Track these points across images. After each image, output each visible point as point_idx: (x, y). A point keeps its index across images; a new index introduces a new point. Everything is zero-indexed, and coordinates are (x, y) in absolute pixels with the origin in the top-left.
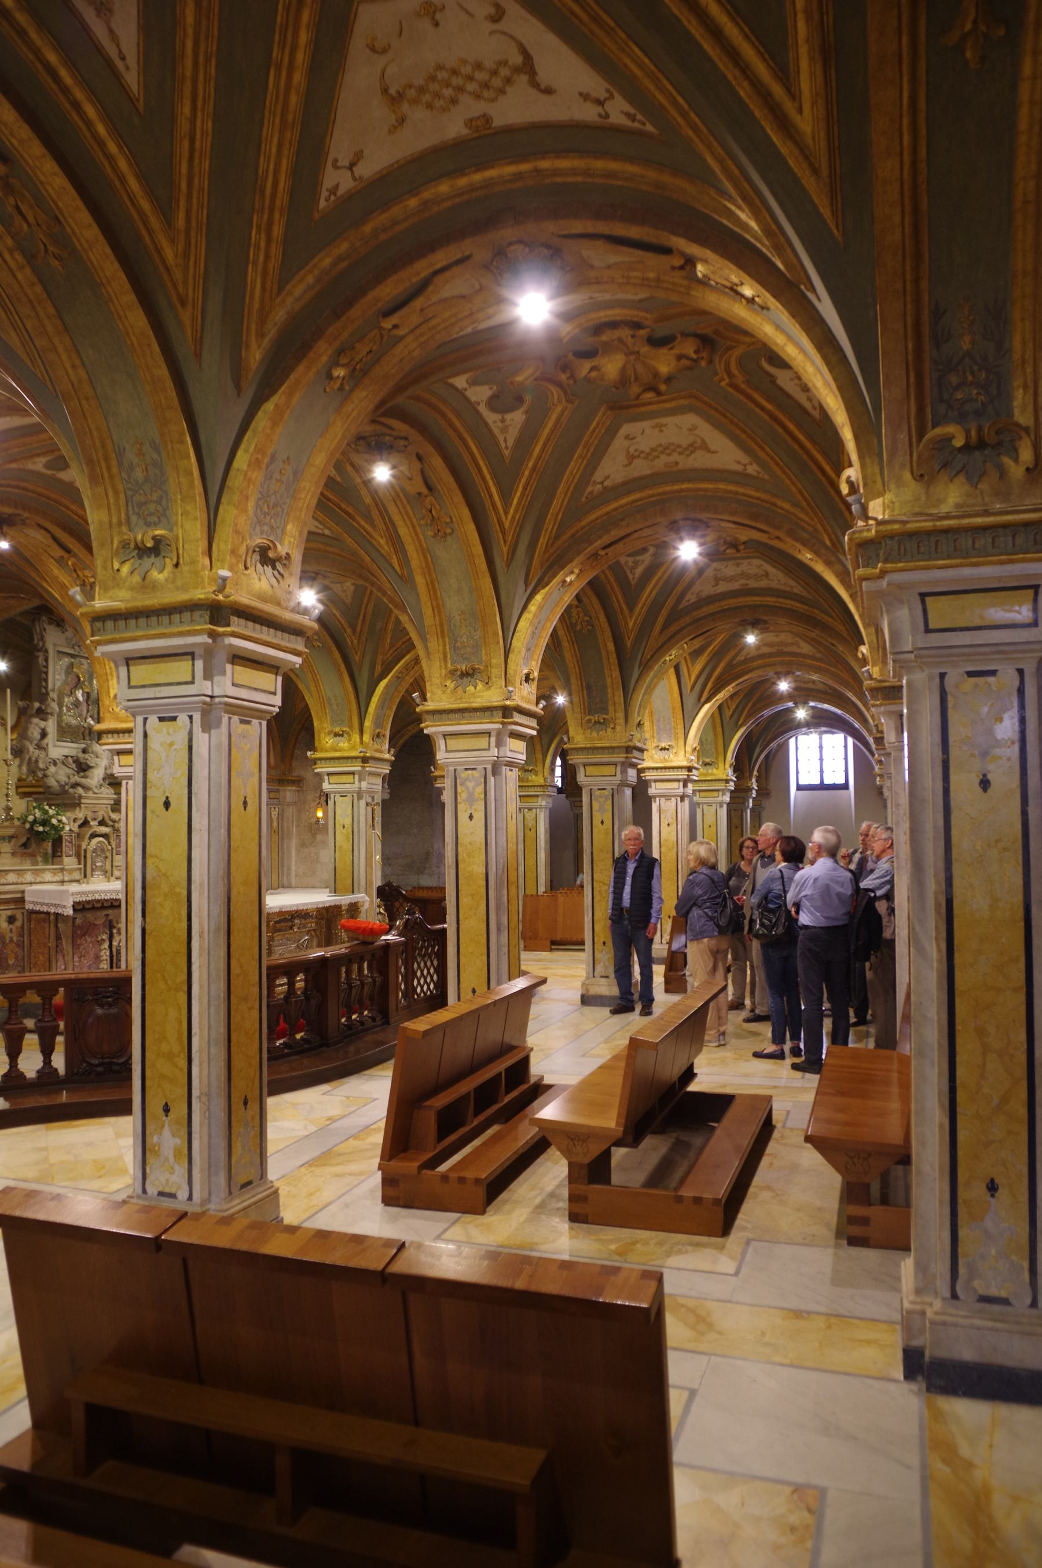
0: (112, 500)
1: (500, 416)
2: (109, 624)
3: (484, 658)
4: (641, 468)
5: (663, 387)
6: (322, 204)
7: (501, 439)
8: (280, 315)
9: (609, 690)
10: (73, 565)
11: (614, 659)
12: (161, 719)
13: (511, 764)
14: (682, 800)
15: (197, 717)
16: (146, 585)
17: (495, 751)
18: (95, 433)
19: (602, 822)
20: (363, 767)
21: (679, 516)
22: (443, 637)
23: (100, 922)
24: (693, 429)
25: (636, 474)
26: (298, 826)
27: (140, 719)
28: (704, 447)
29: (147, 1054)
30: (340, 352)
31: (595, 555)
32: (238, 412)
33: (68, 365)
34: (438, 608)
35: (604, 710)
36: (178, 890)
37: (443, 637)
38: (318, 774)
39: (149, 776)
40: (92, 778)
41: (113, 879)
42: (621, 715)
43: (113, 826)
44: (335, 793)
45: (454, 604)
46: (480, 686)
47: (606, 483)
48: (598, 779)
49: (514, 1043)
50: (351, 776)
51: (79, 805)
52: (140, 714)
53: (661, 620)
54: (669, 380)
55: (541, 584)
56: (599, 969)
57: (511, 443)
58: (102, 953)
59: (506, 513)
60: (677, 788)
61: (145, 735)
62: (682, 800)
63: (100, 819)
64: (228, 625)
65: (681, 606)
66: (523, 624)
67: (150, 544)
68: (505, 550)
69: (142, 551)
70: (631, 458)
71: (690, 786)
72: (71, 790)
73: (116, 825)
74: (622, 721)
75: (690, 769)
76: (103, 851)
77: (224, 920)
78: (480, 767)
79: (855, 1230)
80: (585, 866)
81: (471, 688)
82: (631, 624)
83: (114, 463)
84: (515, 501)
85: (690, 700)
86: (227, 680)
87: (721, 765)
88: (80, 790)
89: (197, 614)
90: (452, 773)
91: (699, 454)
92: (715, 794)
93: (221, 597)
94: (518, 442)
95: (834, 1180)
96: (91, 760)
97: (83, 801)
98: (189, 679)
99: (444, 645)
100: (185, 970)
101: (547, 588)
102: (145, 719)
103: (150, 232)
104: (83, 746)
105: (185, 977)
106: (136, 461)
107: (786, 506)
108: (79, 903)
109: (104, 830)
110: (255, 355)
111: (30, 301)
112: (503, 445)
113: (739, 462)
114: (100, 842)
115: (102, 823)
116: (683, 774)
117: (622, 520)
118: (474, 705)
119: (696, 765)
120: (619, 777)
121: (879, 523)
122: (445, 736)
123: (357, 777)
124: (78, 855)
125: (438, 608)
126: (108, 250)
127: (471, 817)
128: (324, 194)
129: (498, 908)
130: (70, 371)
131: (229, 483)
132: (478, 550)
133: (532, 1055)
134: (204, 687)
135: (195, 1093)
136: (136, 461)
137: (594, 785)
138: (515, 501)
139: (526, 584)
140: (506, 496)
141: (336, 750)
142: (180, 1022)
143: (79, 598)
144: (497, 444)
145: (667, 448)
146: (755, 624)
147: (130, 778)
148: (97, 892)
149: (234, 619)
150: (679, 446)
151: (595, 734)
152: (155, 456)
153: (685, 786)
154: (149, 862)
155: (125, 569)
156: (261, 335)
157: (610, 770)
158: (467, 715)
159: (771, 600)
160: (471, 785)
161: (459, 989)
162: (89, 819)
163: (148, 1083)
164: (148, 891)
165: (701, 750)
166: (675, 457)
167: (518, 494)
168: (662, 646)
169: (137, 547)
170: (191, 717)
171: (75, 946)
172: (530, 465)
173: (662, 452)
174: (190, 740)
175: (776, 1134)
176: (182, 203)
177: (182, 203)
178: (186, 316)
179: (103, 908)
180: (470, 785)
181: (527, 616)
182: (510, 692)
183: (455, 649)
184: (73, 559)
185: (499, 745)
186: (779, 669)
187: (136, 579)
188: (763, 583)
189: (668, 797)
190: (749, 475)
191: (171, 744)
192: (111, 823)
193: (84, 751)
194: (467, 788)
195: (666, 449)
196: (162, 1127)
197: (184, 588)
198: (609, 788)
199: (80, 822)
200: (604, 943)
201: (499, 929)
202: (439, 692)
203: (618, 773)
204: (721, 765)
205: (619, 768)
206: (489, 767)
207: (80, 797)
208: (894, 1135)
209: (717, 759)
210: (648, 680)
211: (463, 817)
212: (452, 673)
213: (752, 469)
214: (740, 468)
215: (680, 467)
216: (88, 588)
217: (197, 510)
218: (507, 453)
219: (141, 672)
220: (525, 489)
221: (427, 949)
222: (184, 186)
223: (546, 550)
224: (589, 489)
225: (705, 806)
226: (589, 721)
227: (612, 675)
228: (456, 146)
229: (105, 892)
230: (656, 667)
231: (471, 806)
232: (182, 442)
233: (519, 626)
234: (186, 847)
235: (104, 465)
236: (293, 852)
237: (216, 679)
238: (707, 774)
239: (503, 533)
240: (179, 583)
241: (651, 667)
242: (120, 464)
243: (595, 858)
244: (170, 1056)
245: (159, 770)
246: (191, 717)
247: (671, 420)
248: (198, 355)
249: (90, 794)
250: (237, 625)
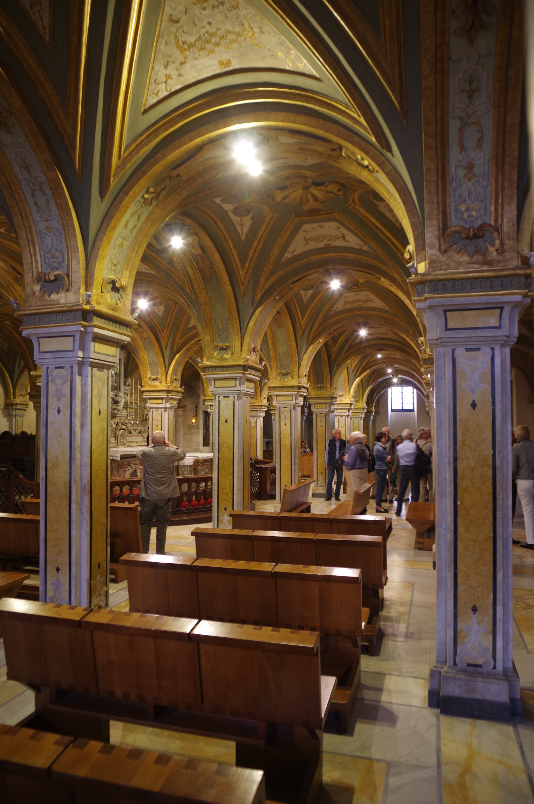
0: (211, 333)
1: (305, 292)
2: (210, 369)
3: (291, 369)
4: (349, 306)
5: (360, 285)
6: (283, 260)
7: (304, 298)
8: (266, 287)
9: (325, 375)
10: (141, 331)
11: (327, 363)
12: (224, 397)
13: (299, 406)
14: (348, 417)
15: (236, 397)
16: (223, 359)
17: (294, 401)
18: (209, 315)
19: (321, 426)
21: (360, 320)
22: (277, 361)
23: (126, 463)
24: (368, 295)
25: (347, 308)
26: (183, 426)
27: (217, 397)
28: (371, 301)
29: (219, 493)
30: (278, 294)
31: (330, 333)
32: (252, 311)
33: (204, 297)
34: (275, 351)
35: (323, 383)
36: (230, 446)
37: (277, 361)
39: (221, 413)
40: (120, 406)
42: (329, 385)
45: (281, 350)
46: (290, 378)
47: (337, 311)
48: (320, 409)
49: (305, 501)
52: (217, 395)
53: (346, 349)
54: (362, 284)
55: (312, 343)
56: (319, 483)
57: (307, 299)
58: (126, 475)
59: (302, 320)
60: (346, 412)
61: (219, 401)
62: (348, 417)
64: (247, 371)
65: (353, 344)
66: (305, 357)
67: (225, 347)
68: (301, 332)
69: (221, 349)
70: (346, 303)
71: (351, 411)
74: (329, 387)
75: (351, 404)
76: (123, 435)
77: (243, 455)
78: (289, 407)
79: (420, 546)
80: (314, 443)
81: (286, 379)
82: (334, 350)
83: (213, 323)
84: (306, 317)
85: (352, 376)
86: (245, 386)
87: (361, 402)
88: (116, 411)
89: (239, 368)
90: (278, 409)
91: (369, 302)
92: (358, 414)
93: (246, 363)
94: (310, 298)
95: (415, 532)
96: (119, 400)
97: (117, 415)
98: (235, 386)
99: (277, 364)
100: (232, 469)
101: (314, 345)
102: (219, 397)
103: (237, 268)
104: (115, 393)
105: (232, 471)
106: (220, 323)
107: (397, 320)
108: (123, 455)
109: (124, 427)
110: (258, 297)
111: (198, 281)
112: (304, 299)
113: (382, 306)
114: (122, 432)
115: (123, 424)
116: (348, 406)
117: (341, 322)
118: (288, 385)
119: (353, 403)
120: (328, 409)
121: (429, 355)
122: (276, 396)
124: (115, 437)
125: (275, 351)
126: (226, 272)
127: (285, 424)
128: (284, 258)
129: (295, 457)
130: (205, 299)
131: (247, 330)
132: (292, 332)
133: (312, 505)
134: (238, 388)
135: (235, 504)
136: (220, 323)
138: (306, 317)
139: (307, 343)
140: (303, 315)
142: (230, 483)
143: (200, 361)
144: (302, 299)
145: (359, 300)
146: (380, 350)
147: (212, 413)
148: (127, 451)
149: (249, 369)
150: (362, 300)
151: (319, 392)
152: (226, 322)
153: (349, 411)
154: (220, 438)
155: (216, 354)
156: (261, 292)
157: (324, 406)
158: (285, 388)
159: (388, 342)
160: (286, 413)
161: (280, 485)
163: (219, 502)
164: (220, 446)
165: (354, 397)
166: (361, 303)
167: (307, 315)
168: (345, 358)
169: (220, 348)
170: (234, 397)
171: (118, 473)
172: (313, 306)
173: (357, 301)
174: (234, 403)
175: (393, 532)
176: (248, 262)
177: (248, 262)
178: (242, 288)
179: (127, 458)
180: (285, 413)
181: (306, 354)
182: (301, 381)
183: (280, 365)
184: (141, 329)
185: (296, 399)
186: (388, 364)
187: (219, 356)
188: (385, 336)
189: (342, 416)
190: (386, 310)
191: (228, 404)
192: (125, 424)
193: (116, 395)
194: (284, 414)
195: (359, 301)
196: (224, 514)
197: (235, 360)
198: (324, 413)
199: (116, 424)
200: (321, 473)
201: (295, 464)
202: (274, 380)
203: (328, 407)
205: (328, 405)
206: (292, 407)
207: (116, 414)
208: (432, 519)
209: (359, 399)
210: (340, 371)
211: (282, 425)
212: (280, 373)
213: (387, 308)
214: (383, 308)
215: (362, 306)
216: (144, 339)
217: (238, 338)
218: (305, 302)
219: (218, 383)
220: (310, 313)
221: (255, 474)
222: (249, 259)
223: (315, 332)
224: (331, 312)
225: (354, 419)
226: (317, 387)
227: (326, 370)
228: (321, 249)
229: (129, 451)
230: (343, 366)
231: (285, 420)
232: (236, 319)
233: (304, 357)
234: (232, 434)
235: (210, 323)
236: (181, 437)
237: (242, 386)
239: (301, 327)
240: (233, 359)
241: (341, 366)
242: (215, 324)
243: (318, 440)
244: (227, 494)
245: (223, 411)
246: (234, 397)
247: (360, 293)
248: (243, 297)
249: (119, 413)
250: (250, 371)
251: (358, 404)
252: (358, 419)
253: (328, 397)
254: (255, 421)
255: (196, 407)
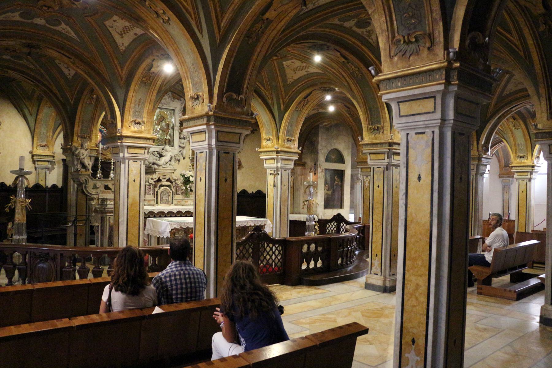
19: (378, 187)
20: (278, 156)
35: (379, 122)
38: (262, 159)
41: (173, 205)
42: (387, 124)
43: (175, 182)
44: (268, 168)
50: (273, 160)
51: (155, 172)
63: (167, 178)
72: (152, 166)
73: (176, 182)
87: (530, 157)
88: (156, 166)
92: (526, 174)
97: (156, 171)
123: (275, 160)
124: (154, 194)
137: (375, 165)
141: (267, 148)
162: (161, 178)
198: (382, 167)
203: (386, 158)
204: (530, 157)
207: (155, 169)
209: (527, 154)
225: (520, 181)
238: (521, 163)
243: (374, 207)
249: (161, 168)
251: (526, 161)
252: (525, 180)
253: (386, 143)
254: (369, 180)
255: (315, 165)
